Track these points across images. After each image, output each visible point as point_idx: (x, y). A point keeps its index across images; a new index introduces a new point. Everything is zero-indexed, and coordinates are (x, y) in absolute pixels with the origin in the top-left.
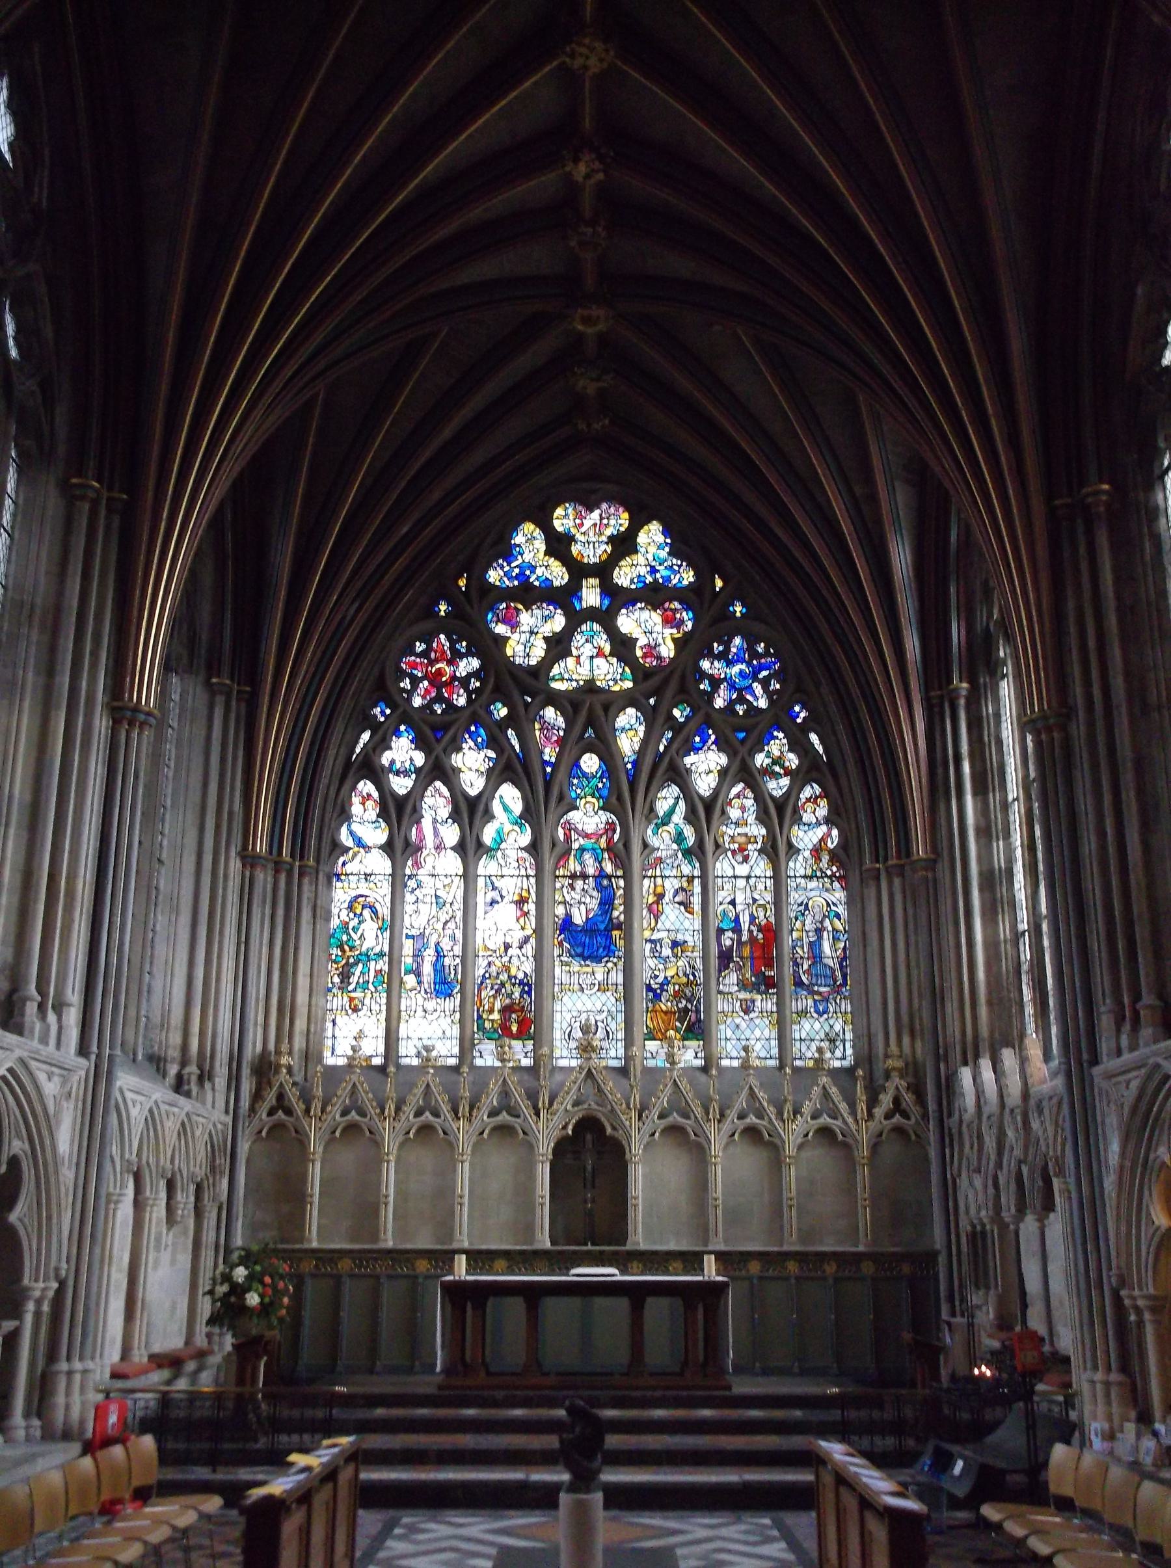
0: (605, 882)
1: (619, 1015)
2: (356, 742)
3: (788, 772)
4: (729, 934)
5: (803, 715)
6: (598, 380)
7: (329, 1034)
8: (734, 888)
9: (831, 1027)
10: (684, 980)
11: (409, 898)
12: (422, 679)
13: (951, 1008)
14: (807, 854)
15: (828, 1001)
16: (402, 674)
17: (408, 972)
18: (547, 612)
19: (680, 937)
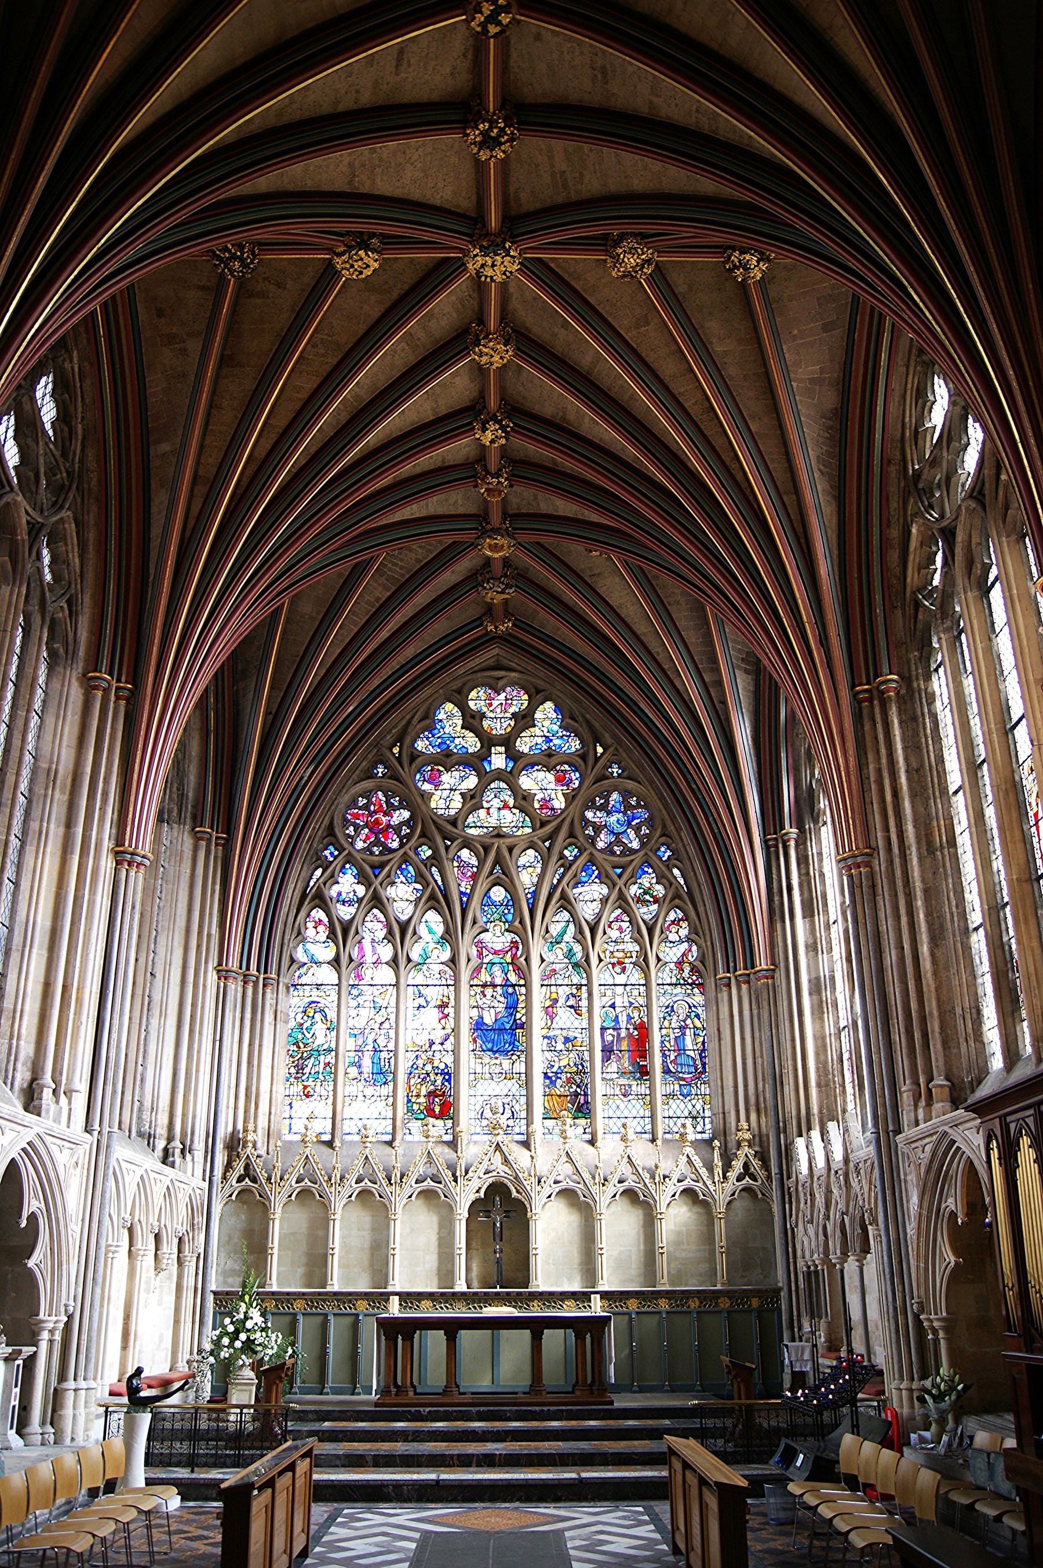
0: (510, 990)
5: (667, 855)
6: (503, 592)
13: (788, 1089)
14: (672, 966)
16: (346, 823)
17: (353, 1064)
19: (571, 1035)
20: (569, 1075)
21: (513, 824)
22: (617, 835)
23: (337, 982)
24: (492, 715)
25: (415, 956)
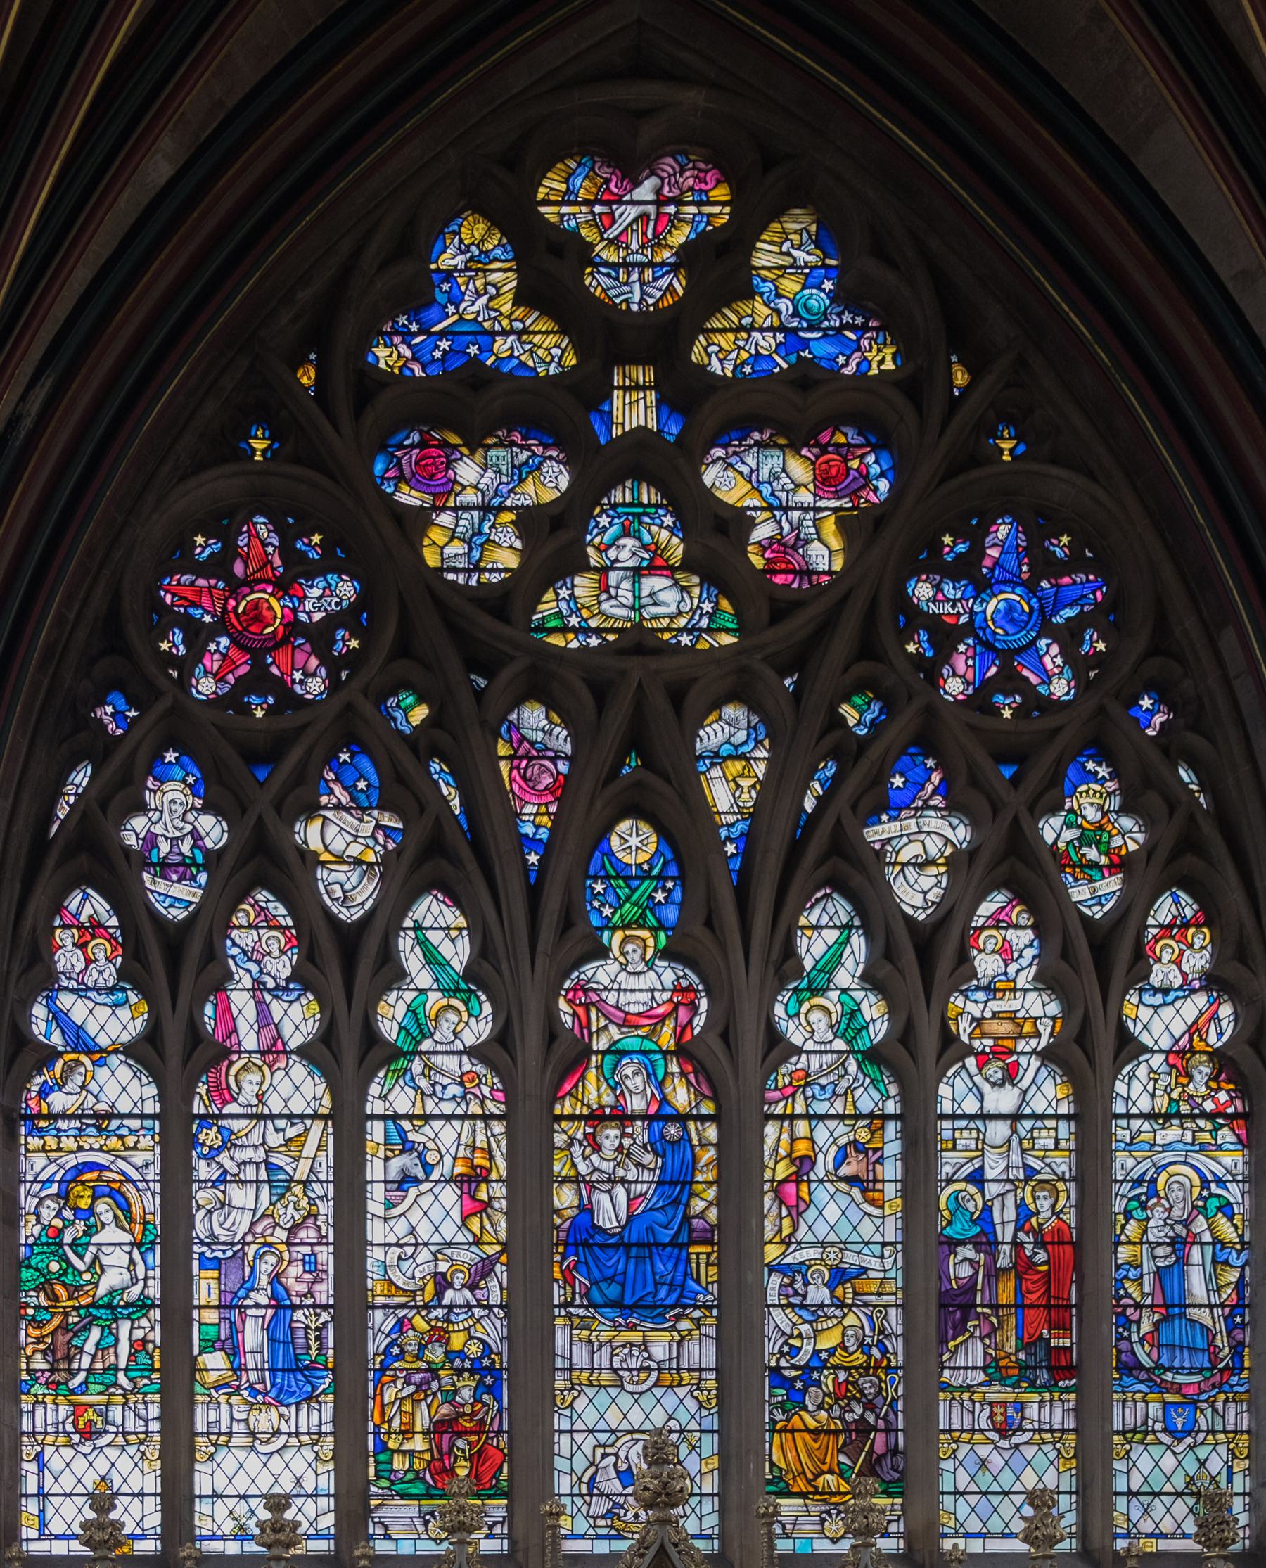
0: (673, 1131)
1: (707, 1439)
2: (57, 793)
3: (1120, 864)
4: (967, 1252)
5: (1159, 719)
7: (31, 1486)
8: (981, 1145)
9: (1202, 1464)
10: (860, 1358)
11: (204, 1170)
14: (1157, 1061)
15: (1195, 1403)
16: (164, 619)
17: (211, 1345)
18: (524, 456)
20: (842, 1376)
21: (682, 622)
22: (1007, 656)
23: (151, 1107)
24: (610, 256)
25: (389, 1030)
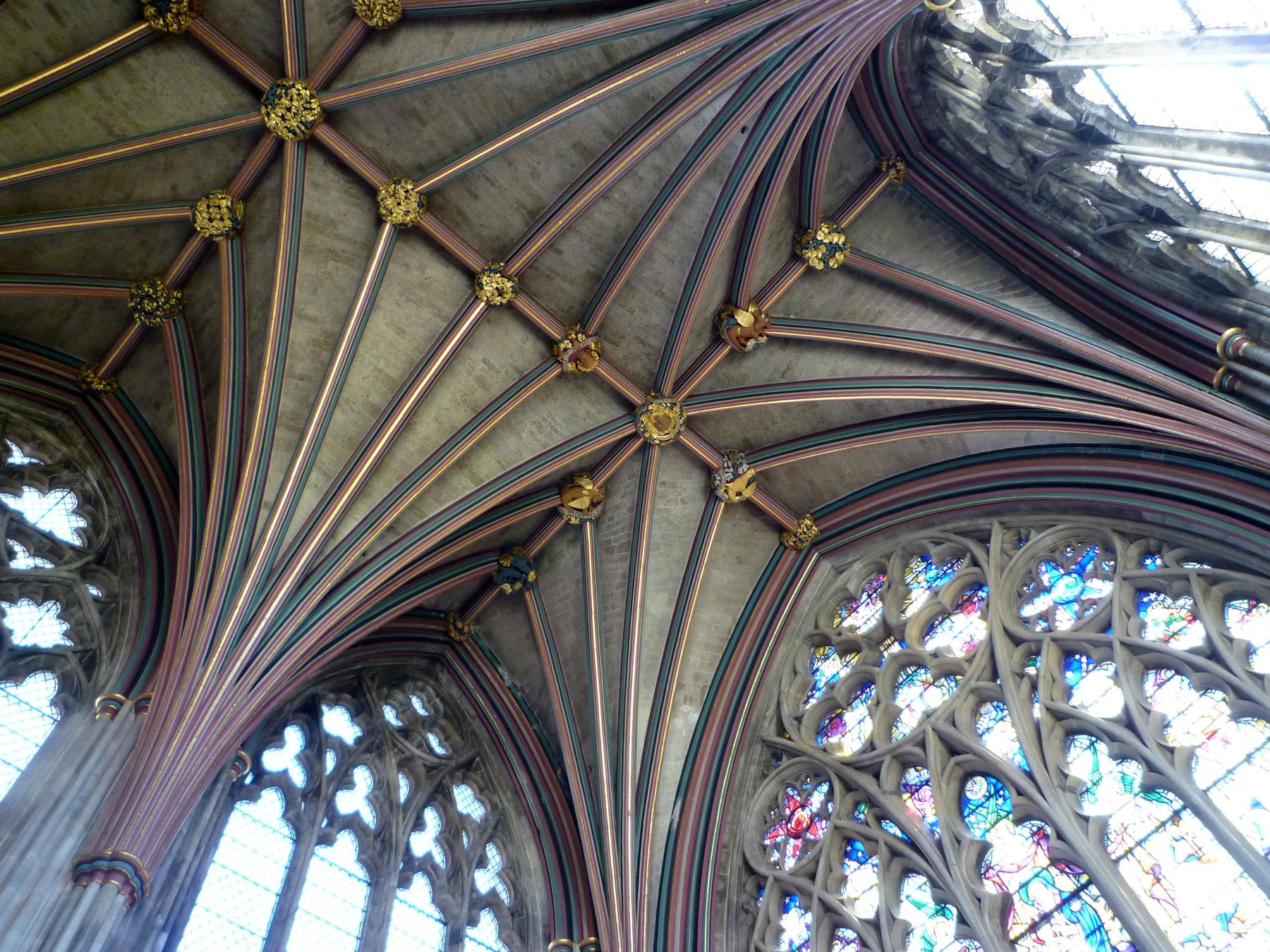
12: (786, 842)
